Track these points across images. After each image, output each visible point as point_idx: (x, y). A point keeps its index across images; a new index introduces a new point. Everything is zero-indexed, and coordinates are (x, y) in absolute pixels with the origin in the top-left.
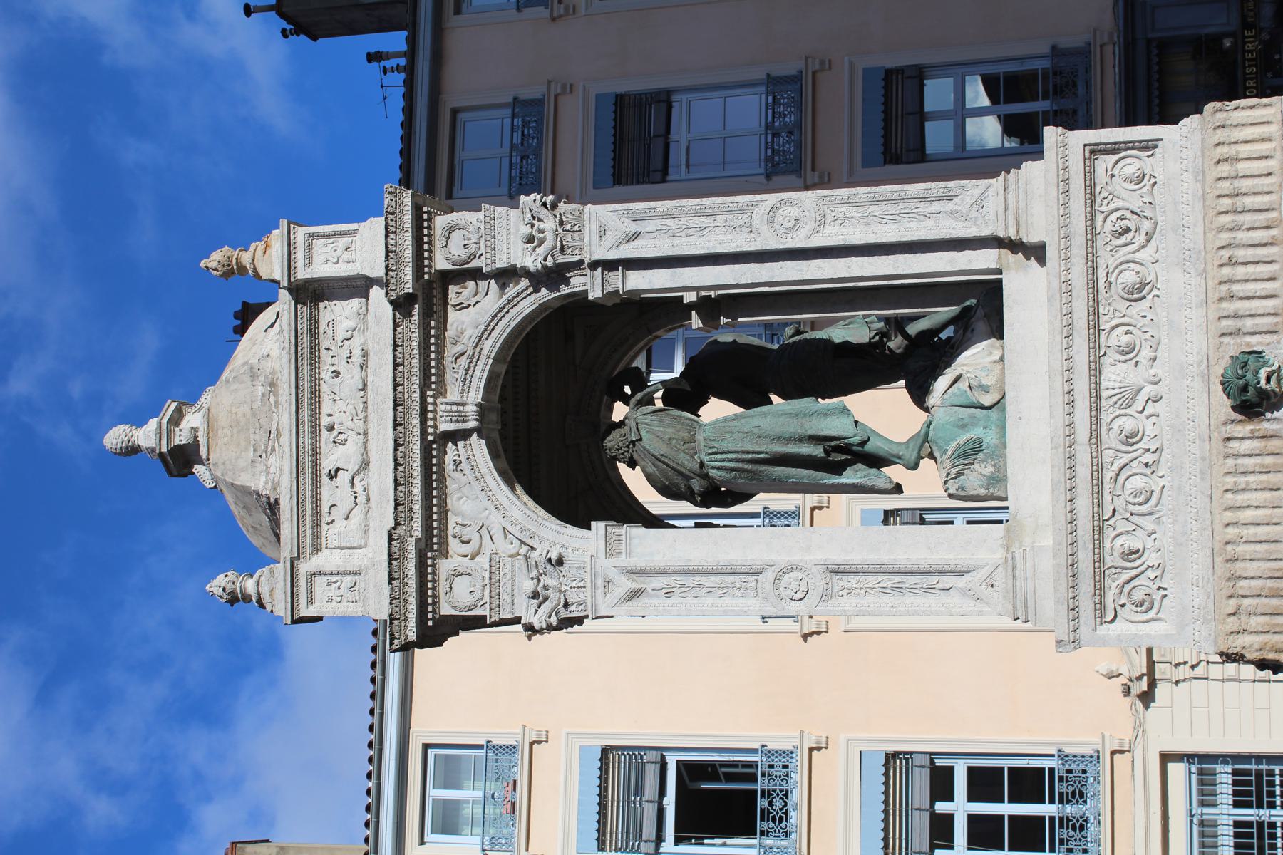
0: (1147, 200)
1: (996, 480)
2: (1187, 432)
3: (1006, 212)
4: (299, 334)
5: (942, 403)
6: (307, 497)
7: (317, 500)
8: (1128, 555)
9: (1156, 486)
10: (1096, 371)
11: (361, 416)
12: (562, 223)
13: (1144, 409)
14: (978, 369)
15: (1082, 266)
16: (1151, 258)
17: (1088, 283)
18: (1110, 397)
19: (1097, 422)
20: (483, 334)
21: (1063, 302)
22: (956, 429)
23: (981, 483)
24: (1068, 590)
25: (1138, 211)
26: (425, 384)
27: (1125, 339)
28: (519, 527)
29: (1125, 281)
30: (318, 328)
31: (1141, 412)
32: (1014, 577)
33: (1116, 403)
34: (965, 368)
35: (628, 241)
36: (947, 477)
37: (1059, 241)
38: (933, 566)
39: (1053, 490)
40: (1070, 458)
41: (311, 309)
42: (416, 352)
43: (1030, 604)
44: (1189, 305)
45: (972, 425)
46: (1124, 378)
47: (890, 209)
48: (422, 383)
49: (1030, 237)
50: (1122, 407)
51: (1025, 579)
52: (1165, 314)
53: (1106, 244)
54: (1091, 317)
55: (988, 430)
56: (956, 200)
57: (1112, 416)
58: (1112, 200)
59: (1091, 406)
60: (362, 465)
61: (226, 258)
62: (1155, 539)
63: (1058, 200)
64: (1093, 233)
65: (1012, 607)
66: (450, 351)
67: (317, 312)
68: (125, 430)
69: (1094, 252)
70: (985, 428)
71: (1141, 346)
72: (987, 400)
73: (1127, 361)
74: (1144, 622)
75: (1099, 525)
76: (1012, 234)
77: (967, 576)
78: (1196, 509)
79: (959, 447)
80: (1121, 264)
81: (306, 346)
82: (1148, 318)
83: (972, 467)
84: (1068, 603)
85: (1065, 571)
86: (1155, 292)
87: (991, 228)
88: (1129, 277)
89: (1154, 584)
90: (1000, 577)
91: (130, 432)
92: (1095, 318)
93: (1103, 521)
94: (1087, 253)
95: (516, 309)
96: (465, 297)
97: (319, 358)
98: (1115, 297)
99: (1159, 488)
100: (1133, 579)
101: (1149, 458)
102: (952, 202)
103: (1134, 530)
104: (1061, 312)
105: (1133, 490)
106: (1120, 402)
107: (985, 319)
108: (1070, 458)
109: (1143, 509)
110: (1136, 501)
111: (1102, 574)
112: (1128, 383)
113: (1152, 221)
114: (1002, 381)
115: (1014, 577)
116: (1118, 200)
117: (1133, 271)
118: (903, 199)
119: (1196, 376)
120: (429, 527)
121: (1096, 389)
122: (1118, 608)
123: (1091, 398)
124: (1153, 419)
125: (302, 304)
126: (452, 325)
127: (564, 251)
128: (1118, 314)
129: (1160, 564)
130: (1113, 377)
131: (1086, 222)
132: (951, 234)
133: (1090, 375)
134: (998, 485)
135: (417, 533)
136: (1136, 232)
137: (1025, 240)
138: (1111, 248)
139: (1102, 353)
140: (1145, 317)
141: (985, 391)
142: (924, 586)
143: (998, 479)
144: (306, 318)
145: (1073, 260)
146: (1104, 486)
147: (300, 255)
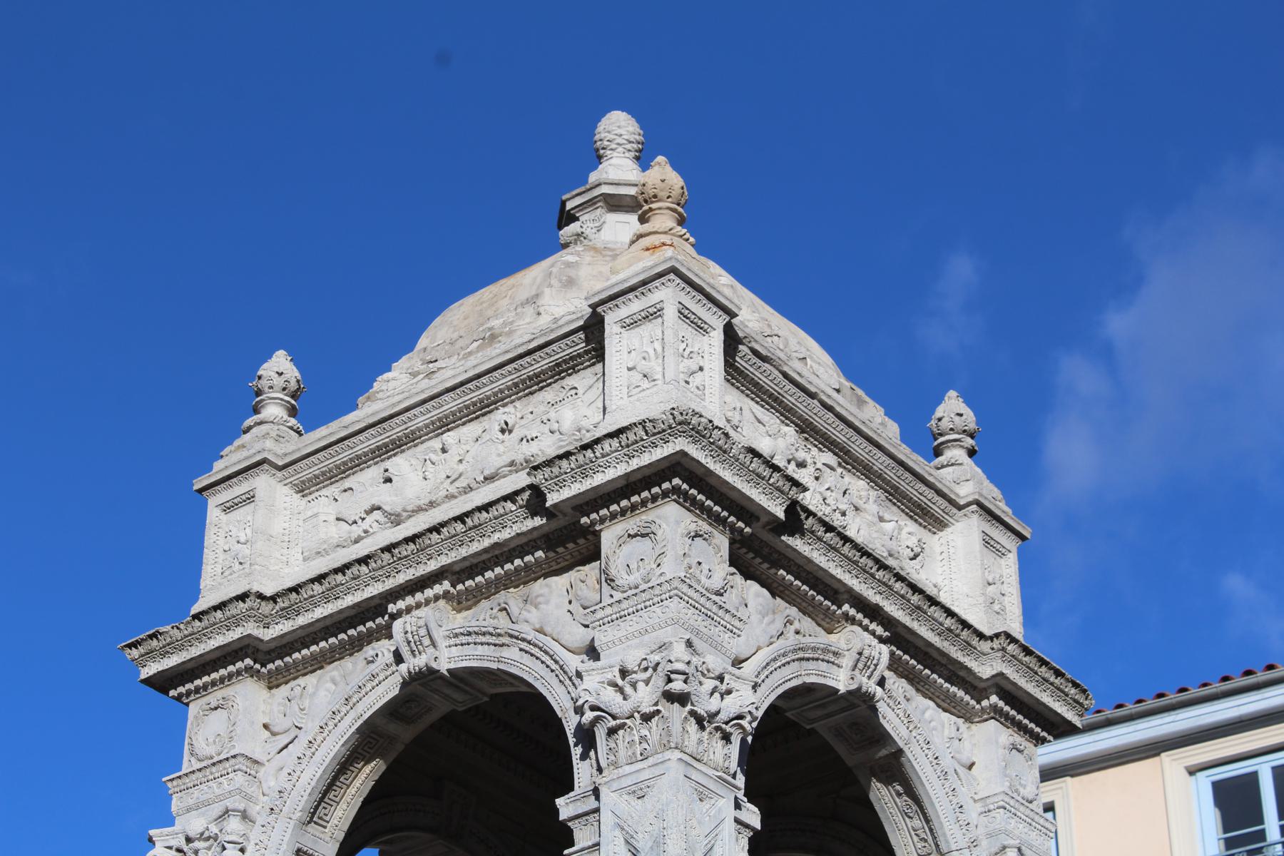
4: (546, 350)
6: (355, 450)
7: (358, 465)
11: (452, 489)
12: (647, 718)
20: (523, 640)
26: (458, 573)
28: (288, 786)
30: (570, 375)
35: (627, 842)
41: (586, 352)
42: (486, 543)
48: (457, 568)
60: (393, 515)
61: (651, 193)
66: (511, 597)
67: (588, 363)
68: (621, 135)
81: (535, 367)
91: (618, 144)
95: (555, 682)
96: (579, 593)
97: (531, 393)
120: (291, 648)
125: (586, 337)
126: (547, 585)
127: (610, 736)
144: (571, 350)
147: (634, 306)
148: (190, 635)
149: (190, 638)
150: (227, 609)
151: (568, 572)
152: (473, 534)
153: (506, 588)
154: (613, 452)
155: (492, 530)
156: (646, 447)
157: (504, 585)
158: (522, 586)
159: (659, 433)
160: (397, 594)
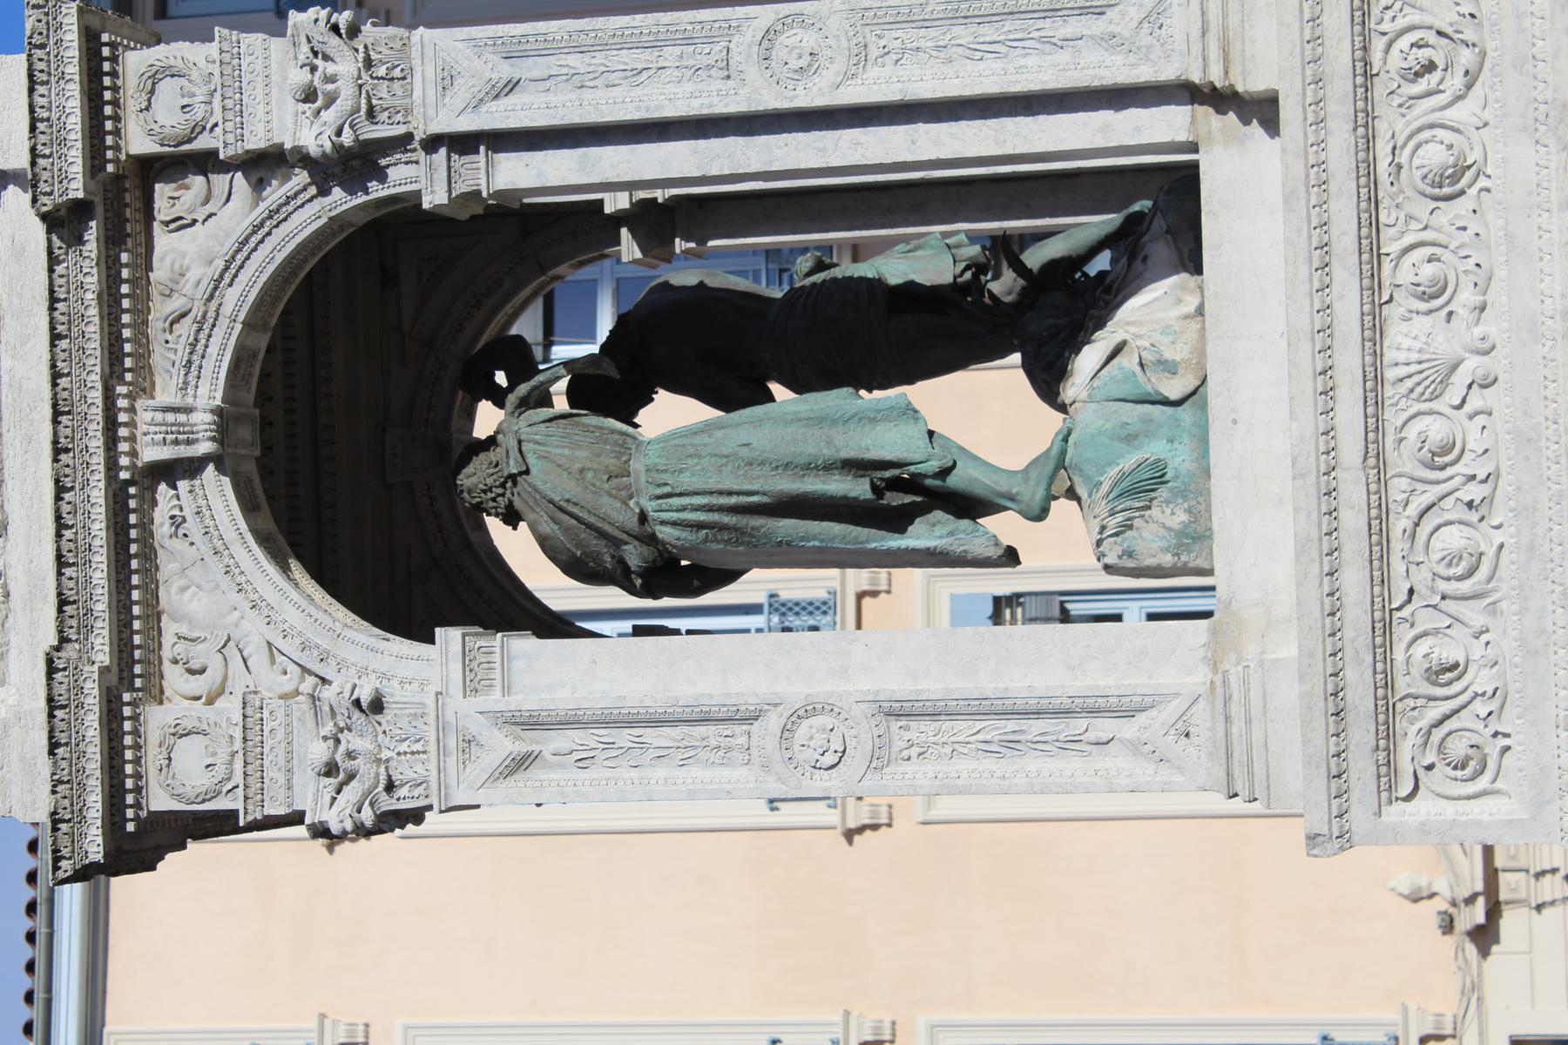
0: (1466, 10)
1: (1193, 538)
2: (1543, 443)
3: (1204, 35)
5: (1090, 396)
8: (1437, 673)
9: (1486, 541)
10: (1374, 330)
12: (369, 63)
13: (1464, 401)
14: (1154, 330)
15: (1347, 136)
16: (1474, 119)
17: (1358, 167)
18: (1401, 380)
19: (1377, 428)
20: (221, 276)
21: (1313, 203)
22: (1116, 444)
23: (1164, 544)
24: (1327, 741)
25: (1449, 31)
26: (112, 373)
27: (1428, 271)
29: (1426, 162)
31: (1459, 407)
32: (1228, 719)
33: (1412, 391)
34: (1132, 329)
35: (497, 96)
36: (1101, 532)
37: (1304, 89)
38: (1077, 700)
39: (1298, 556)
40: (1328, 494)
42: (93, 311)
43: (1259, 768)
44: (1545, 206)
45: (1146, 436)
46: (1425, 343)
47: (989, 32)
48: (107, 370)
49: (1251, 83)
50: (1424, 398)
51: (1249, 721)
52: (1501, 222)
53: (1392, 93)
54: (1364, 231)
55: (1176, 445)
56: (1111, 13)
57: (1405, 415)
58: (1401, 10)
59: (1366, 397)
62: (1488, 643)
63: (1301, 11)
64: (1366, 74)
65: (1224, 774)
66: (160, 310)
69: (1369, 108)
70: (1171, 441)
71: (1457, 285)
72: (1173, 390)
73: (1431, 311)
74: (1469, 798)
75: (1383, 619)
76: (1216, 77)
77: (1141, 718)
78: (1562, 585)
79: (1123, 476)
80: (1419, 130)
82: (1470, 232)
83: (1147, 513)
84: (1328, 764)
85: (1321, 704)
86: (1483, 182)
87: (1176, 65)
88: (1434, 156)
89: (1486, 726)
90: (1202, 716)
92: (1371, 232)
93: (1391, 610)
94: (1356, 112)
95: (285, 228)
96: (186, 207)
98: (1410, 192)
99: (1494, 549)
100: (1447, 717)
101: (1474, 492)
102: (1103, 17)
103: (1449, 627)
104: (1309, 222)
105: (1446, 553)
106: (1419, 389)
107: (1169, 237)
108: (1328, 494)
109: (1465, 587)
110: (1452, 572)
111: (1390, 710)
112: (1434, 353)
113: (1477, 50)
114: (1201, 352)
115: (1228, 719)
116: (1413, 10)
117: (1442, 143)
118: (1012, 13)
119: (1559, 339)
120: (125, 645)
121: (1374, 364)
122: (1421, 773)
123: (1365, 382)
124: (1481, 420)
126: (162, 259)
127: (374, 117)
128: (1414, 225)
129: (1497, 688)
130: (1406, 343)
131: (1353, 52)
132: (1102, 78)
133: (1363, 340)
134: (1197, 547)
135: (103, 656)
136: (1445, 70)
137: (1240, 88)
138: (1400, 100)
139: (1385, 298)
140: (1464, 229)
141: (1169, 372)
142: (1061, 737)
143: (1196, 535)
145: (1330, 123)
146: (1391, 545)
148: (71, 766)
149: (74, 768)
150: (56, 698)
151: (153, 237)
152: (76, 329)
153: (146, 322)
154: (50, 96)
155: (80, 302)
156: (58, 53)
157: (143, 323)
158: (151, 304)
159: (48, 29)
160: (112, 460)
